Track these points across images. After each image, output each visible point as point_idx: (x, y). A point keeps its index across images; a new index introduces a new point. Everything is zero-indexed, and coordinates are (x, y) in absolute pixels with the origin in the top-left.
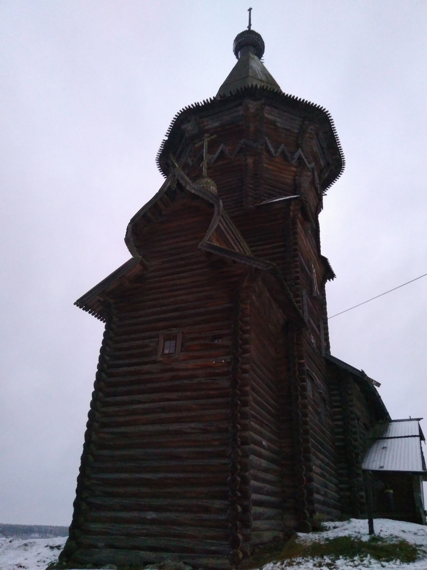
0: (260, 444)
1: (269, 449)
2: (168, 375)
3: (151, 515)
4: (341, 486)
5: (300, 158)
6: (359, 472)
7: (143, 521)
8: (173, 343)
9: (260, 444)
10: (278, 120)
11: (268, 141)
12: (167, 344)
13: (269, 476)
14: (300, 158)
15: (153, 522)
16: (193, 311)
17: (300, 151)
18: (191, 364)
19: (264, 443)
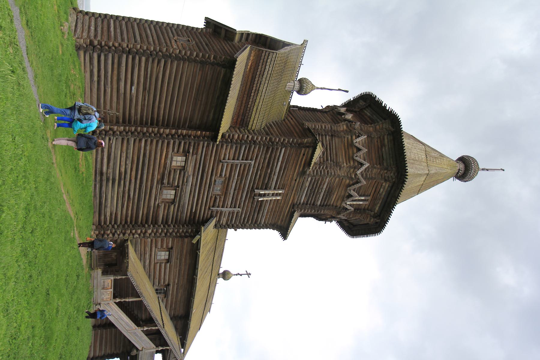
0: (132, 84)
9: (132, 84)
10: (387, 148)
14: (362, 165)
19: (133, 88)
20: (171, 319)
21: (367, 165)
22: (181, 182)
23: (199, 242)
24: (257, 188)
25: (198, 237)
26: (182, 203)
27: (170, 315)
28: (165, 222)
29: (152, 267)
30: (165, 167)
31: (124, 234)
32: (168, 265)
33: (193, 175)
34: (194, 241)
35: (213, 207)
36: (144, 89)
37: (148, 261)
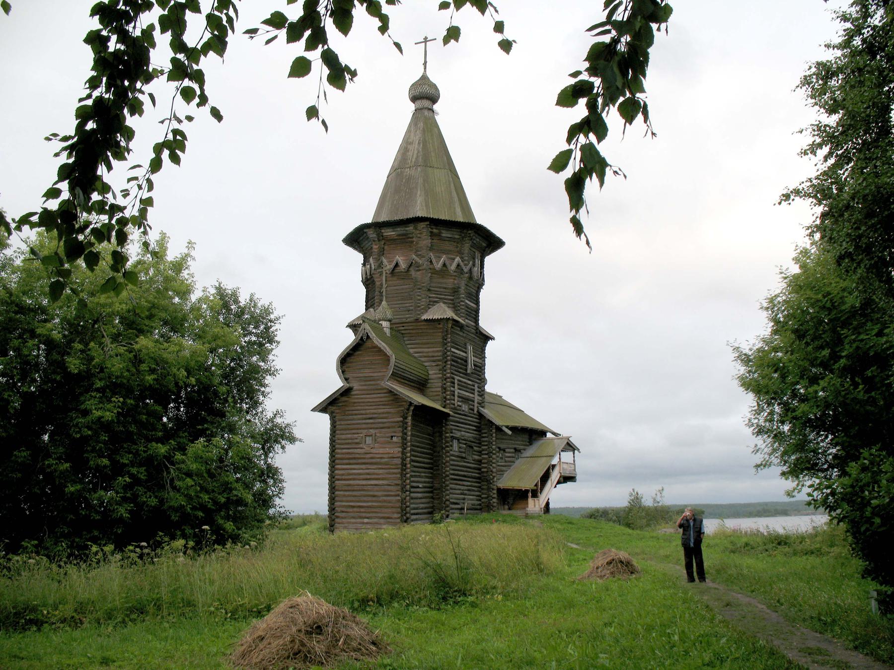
0: (418, 487)
1: (425, 487)
2: (368, 456)
3: (366, 520)
4: (483, 496)
5: (458, 265)
6: (495, 487)
7: (363, 523)
8: (371, 438)
9: (418, 487)
11: (433, 257)
12: (367, 438)
13: (424, 500)
15: (367, 523)
16: (380, 420)
17: (458, 259)
18: (381, 451)
20: (531, 444)
21: (458, 259)
22: (464, 442)
23: (507, 427)
24: (466, 370)
25: (504, 429)
26: (472, 440)
27: (528, 446)
28: (480, 453)
29: (506, 464)
30: (458, 456)
31: (493, 489)
32: (507, 450)
33: (461, 431)
34: (510, 432)
35: (473, 410)
36: (420, 476)
37: (504, 468)
